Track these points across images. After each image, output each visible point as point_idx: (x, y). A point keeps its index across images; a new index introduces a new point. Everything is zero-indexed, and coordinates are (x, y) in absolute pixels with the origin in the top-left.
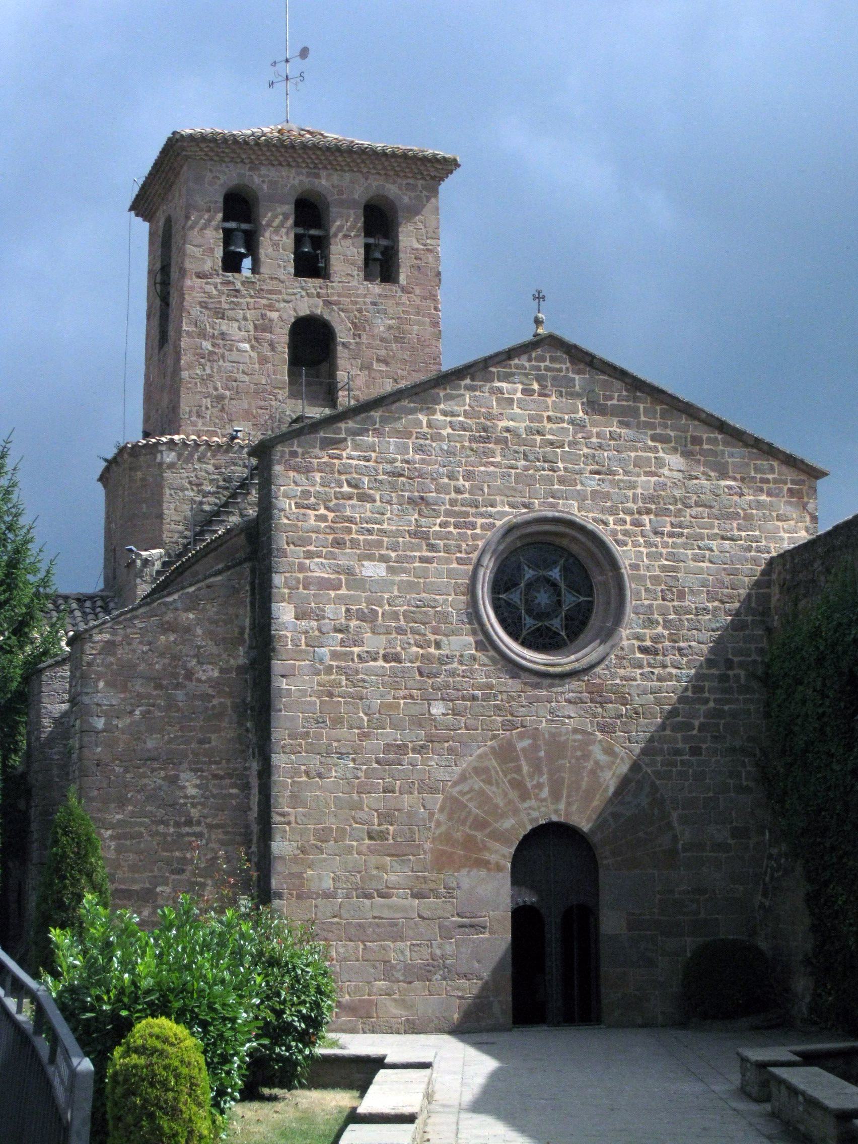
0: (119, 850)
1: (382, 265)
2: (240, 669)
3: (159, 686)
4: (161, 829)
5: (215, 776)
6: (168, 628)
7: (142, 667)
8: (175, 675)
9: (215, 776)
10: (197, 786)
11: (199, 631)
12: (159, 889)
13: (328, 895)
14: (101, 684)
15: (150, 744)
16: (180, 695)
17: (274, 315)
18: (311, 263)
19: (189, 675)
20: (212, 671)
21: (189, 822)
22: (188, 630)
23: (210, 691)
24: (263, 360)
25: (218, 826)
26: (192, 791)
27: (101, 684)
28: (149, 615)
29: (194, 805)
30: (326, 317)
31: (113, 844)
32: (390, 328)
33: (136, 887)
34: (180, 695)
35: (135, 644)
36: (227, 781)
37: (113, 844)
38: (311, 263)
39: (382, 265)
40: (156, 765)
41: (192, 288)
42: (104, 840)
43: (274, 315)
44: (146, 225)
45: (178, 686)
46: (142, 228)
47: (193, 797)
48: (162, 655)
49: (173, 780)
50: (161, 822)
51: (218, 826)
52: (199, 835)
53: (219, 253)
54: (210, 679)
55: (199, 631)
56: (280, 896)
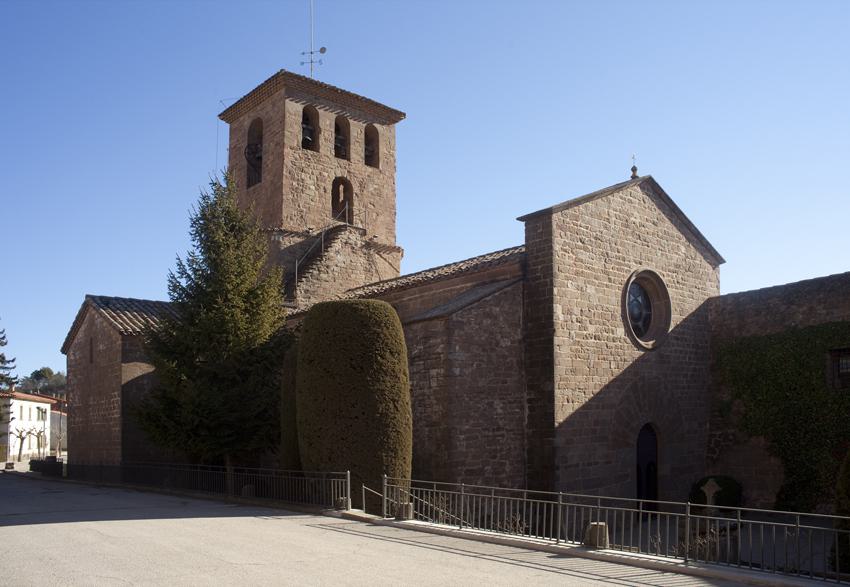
0: (467, 447)
1: (371, 158)
2: (520, 342)
3: (484, 350)
4: (486, 433)
5: (510, 403)
6: (489, 315)
7: (476, 338)
8: (491, 344)
9: (510, 403)
10: (501, 408)
11: (501, 319)
12: (486, 468)
13: (577, 465)
14: (457, 348)
15: (480, 384)
16: (493, 355)
17: (326, 174)
18: (342, 150)
19: (497, 344)
20: (509, 340)
21: (499, 429)
22: (496, 318)
23: (506, 353)
24: (321, 196)
25: (511, 430)
26: (500, 411)
27: (457, 348)
28: (478, 307)
29: (501, 419)
30: (348, 178)
31: (465, 443)
32: (375, 189)
33: (475, 468)
34: (493, 355)
35: (473, 325)
36: (515, 405)
37: (465, 443)
38: (342, 150)
39: (371, 158)
40: (483, 396)
41: (288, 154)
42: (459, 441)
43: (326, 174)
44: (228, 125)
45: (493, 350)
46: (225, 127)
47: (500, 414)
48: (485, 331)
49: (491, 405)
50: (486, 429)
51: (511, 430)
52: (503, 436)
53: (301, 139)
54: (506, 347)
55: (501, 319)
56: (558, 468)
